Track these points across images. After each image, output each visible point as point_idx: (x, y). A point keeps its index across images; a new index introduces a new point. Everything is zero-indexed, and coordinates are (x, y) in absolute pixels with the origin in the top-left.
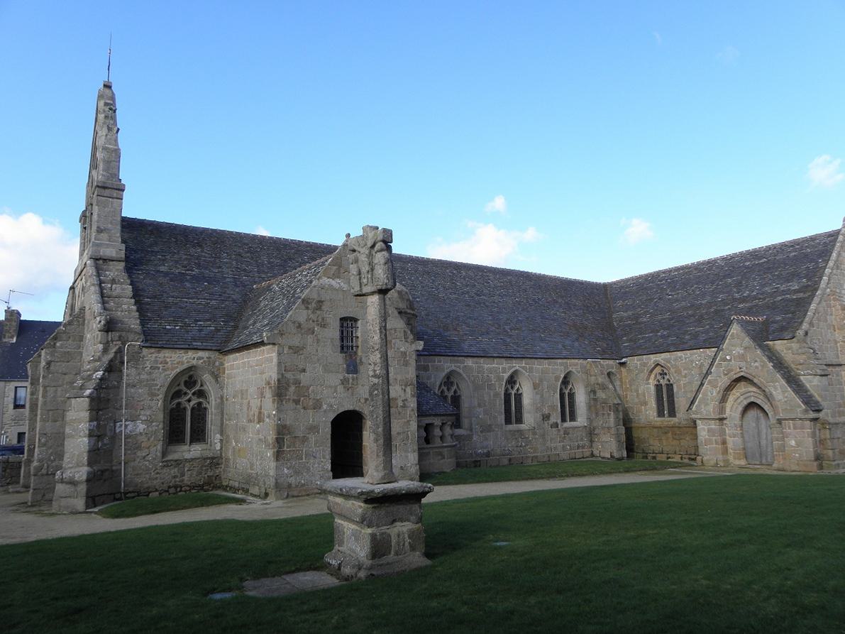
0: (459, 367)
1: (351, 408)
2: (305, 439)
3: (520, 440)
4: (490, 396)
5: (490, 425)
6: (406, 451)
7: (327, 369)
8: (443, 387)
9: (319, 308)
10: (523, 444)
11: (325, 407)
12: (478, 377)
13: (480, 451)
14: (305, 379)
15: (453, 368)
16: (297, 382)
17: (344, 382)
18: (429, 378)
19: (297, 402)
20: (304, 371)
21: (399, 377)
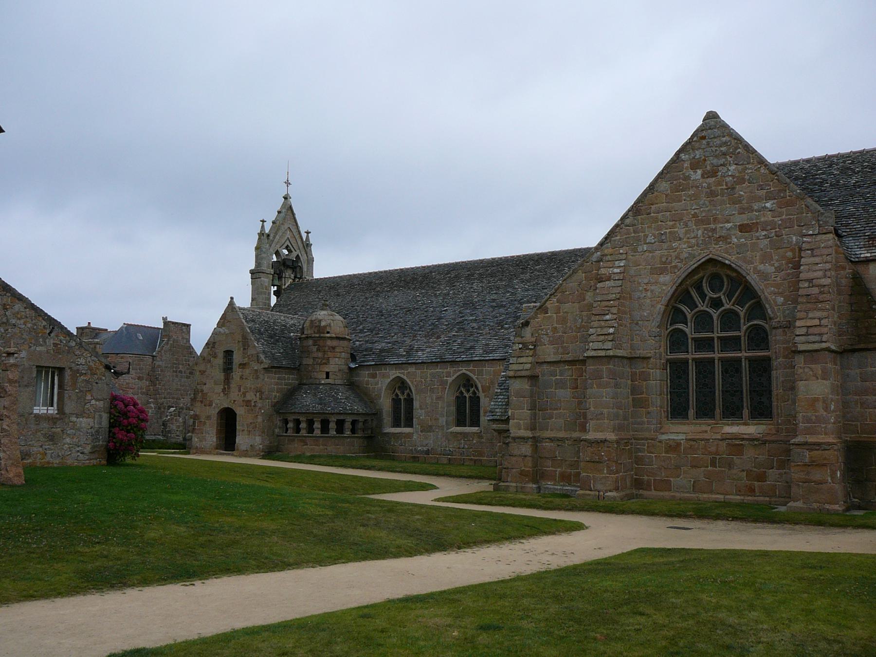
0: (403, 373)
1: (226, 406)
2: (205, 423)
3: (462, 441)
4: (432, 399)
5: (431, 426)
6: (255, 435)
7: (216, 383)
8: (397, 391)
9: (213, 347)
10: (466, 446)
11: (214, 405)
12: (422, 382)
13: (419, 448)
14: (205, 388)
15: (464, 371)
16: (202, 391)
17: (224, 390)
18: (377, 384)
19: (202, 402)
20: (205, 384)
21: (253, 387)
